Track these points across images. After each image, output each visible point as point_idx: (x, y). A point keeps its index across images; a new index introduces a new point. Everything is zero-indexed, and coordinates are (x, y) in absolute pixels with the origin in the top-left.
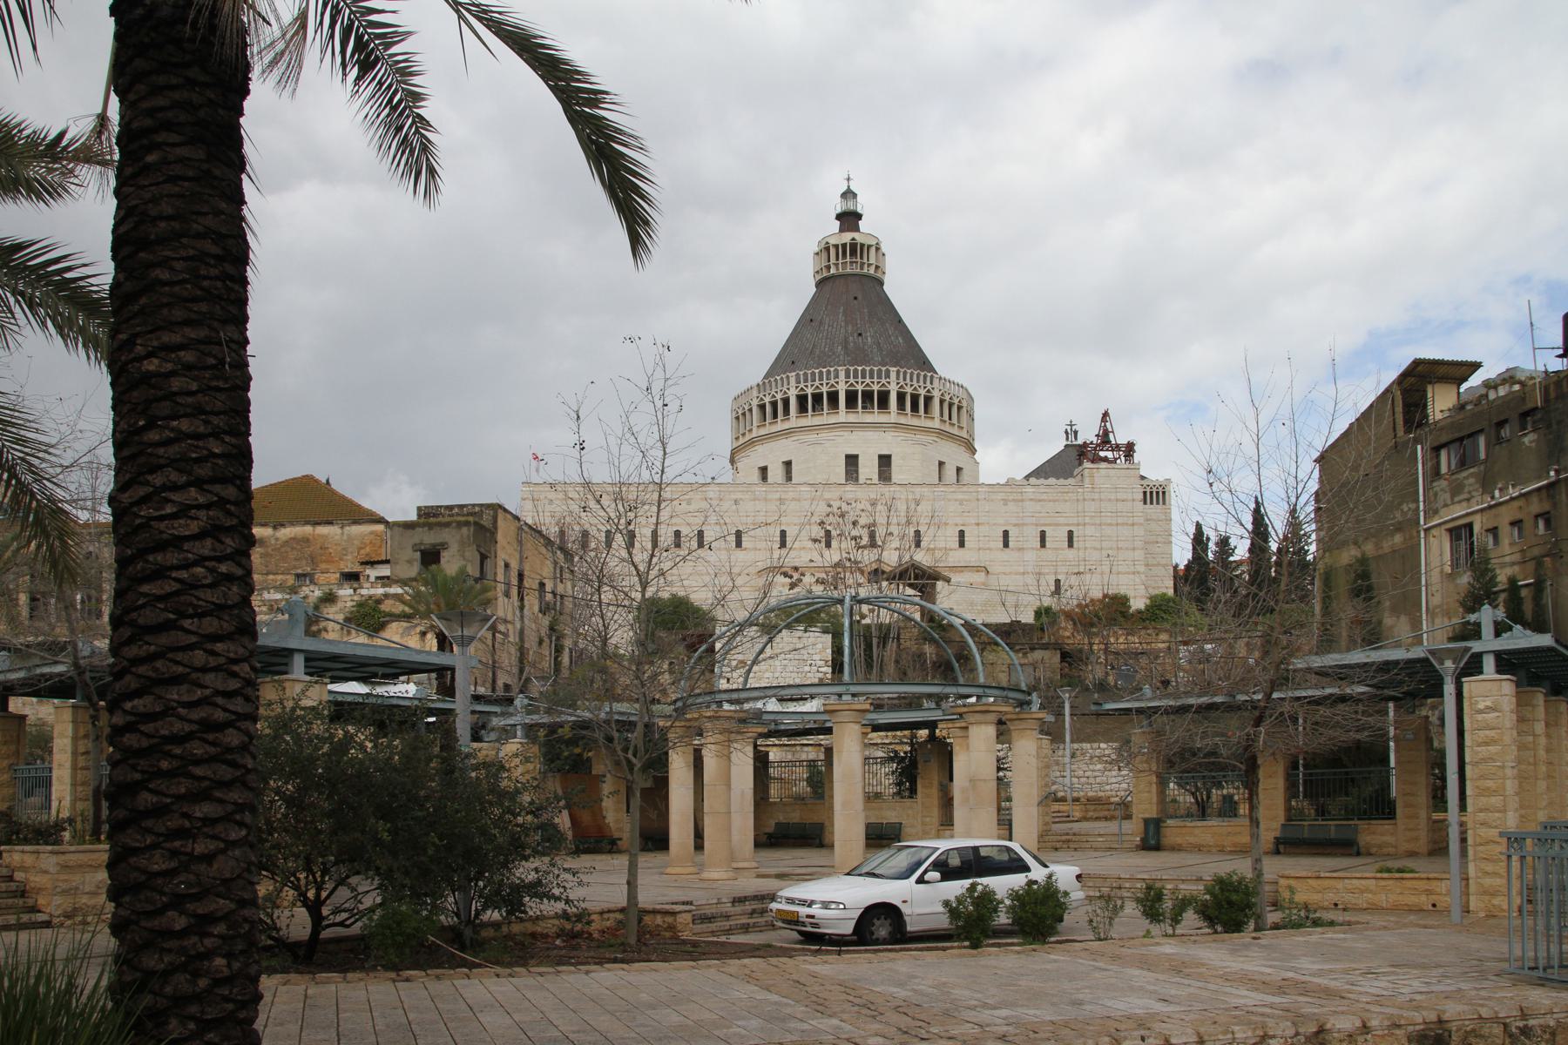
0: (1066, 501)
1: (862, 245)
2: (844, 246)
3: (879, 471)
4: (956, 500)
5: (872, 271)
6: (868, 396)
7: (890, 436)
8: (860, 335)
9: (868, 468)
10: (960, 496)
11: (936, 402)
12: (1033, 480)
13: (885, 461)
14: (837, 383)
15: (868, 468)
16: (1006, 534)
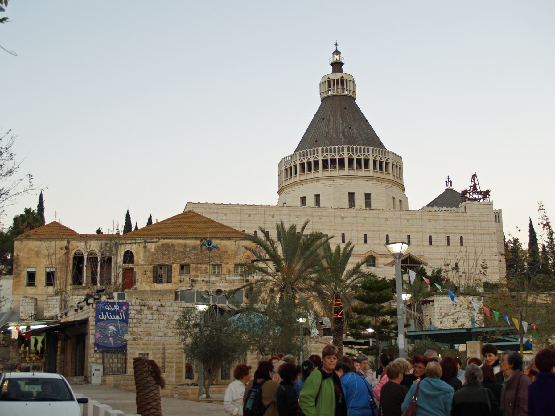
0: (459, 221)
1: (347, 80)
2: (338, 80)
3: (365, 201)
4: (406, 219)
5: (351, 94)
6: (333, 161)
7: (370, 183)
8: (350, 128)
9: (360, 200)
10: (408, 217)
11: (390, 165)
12: (430, 208)
13: (368, 196)
14: (318, 156)
15: (360, 200)
16: (430, 237)
